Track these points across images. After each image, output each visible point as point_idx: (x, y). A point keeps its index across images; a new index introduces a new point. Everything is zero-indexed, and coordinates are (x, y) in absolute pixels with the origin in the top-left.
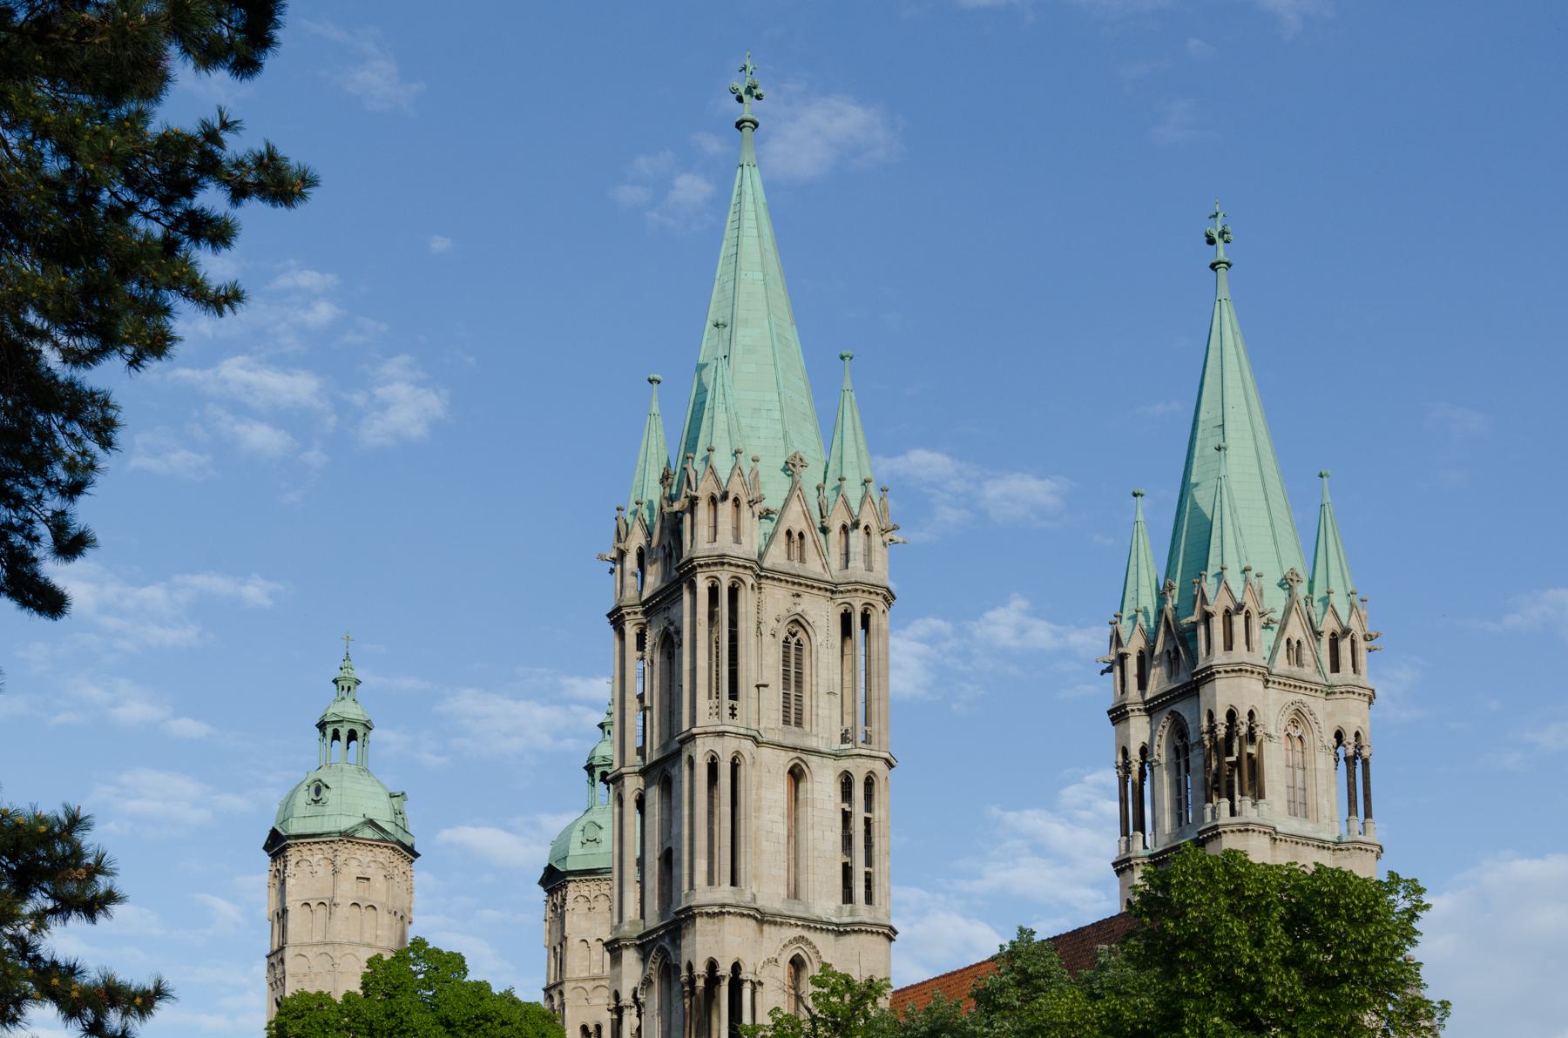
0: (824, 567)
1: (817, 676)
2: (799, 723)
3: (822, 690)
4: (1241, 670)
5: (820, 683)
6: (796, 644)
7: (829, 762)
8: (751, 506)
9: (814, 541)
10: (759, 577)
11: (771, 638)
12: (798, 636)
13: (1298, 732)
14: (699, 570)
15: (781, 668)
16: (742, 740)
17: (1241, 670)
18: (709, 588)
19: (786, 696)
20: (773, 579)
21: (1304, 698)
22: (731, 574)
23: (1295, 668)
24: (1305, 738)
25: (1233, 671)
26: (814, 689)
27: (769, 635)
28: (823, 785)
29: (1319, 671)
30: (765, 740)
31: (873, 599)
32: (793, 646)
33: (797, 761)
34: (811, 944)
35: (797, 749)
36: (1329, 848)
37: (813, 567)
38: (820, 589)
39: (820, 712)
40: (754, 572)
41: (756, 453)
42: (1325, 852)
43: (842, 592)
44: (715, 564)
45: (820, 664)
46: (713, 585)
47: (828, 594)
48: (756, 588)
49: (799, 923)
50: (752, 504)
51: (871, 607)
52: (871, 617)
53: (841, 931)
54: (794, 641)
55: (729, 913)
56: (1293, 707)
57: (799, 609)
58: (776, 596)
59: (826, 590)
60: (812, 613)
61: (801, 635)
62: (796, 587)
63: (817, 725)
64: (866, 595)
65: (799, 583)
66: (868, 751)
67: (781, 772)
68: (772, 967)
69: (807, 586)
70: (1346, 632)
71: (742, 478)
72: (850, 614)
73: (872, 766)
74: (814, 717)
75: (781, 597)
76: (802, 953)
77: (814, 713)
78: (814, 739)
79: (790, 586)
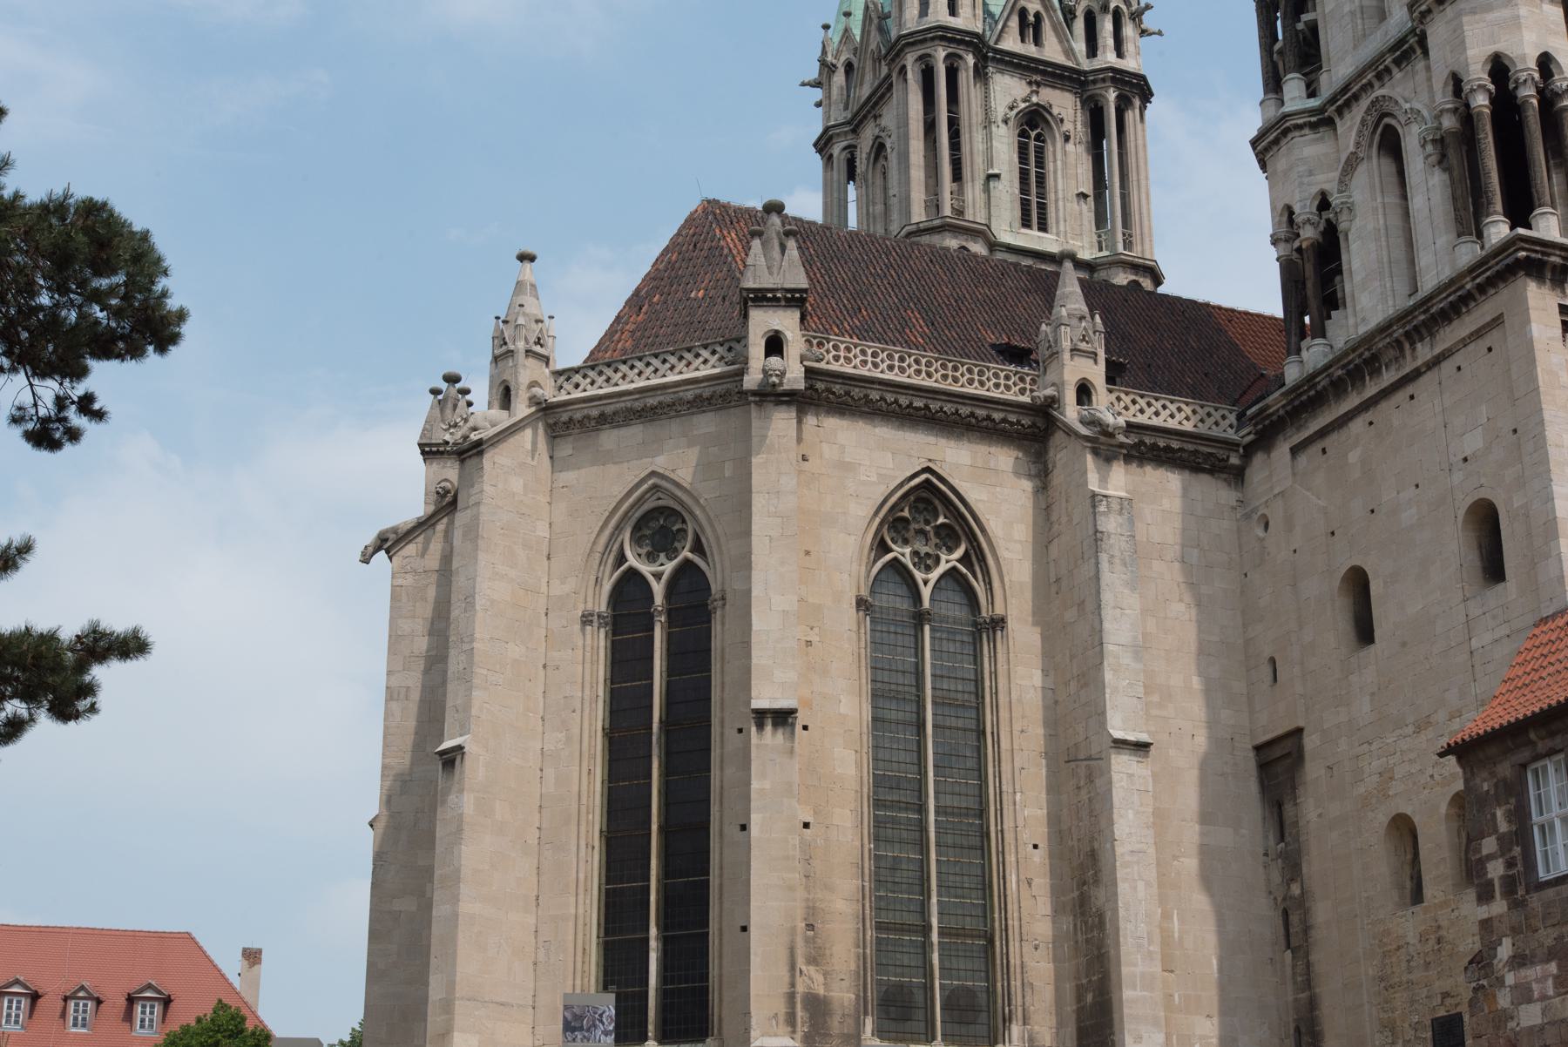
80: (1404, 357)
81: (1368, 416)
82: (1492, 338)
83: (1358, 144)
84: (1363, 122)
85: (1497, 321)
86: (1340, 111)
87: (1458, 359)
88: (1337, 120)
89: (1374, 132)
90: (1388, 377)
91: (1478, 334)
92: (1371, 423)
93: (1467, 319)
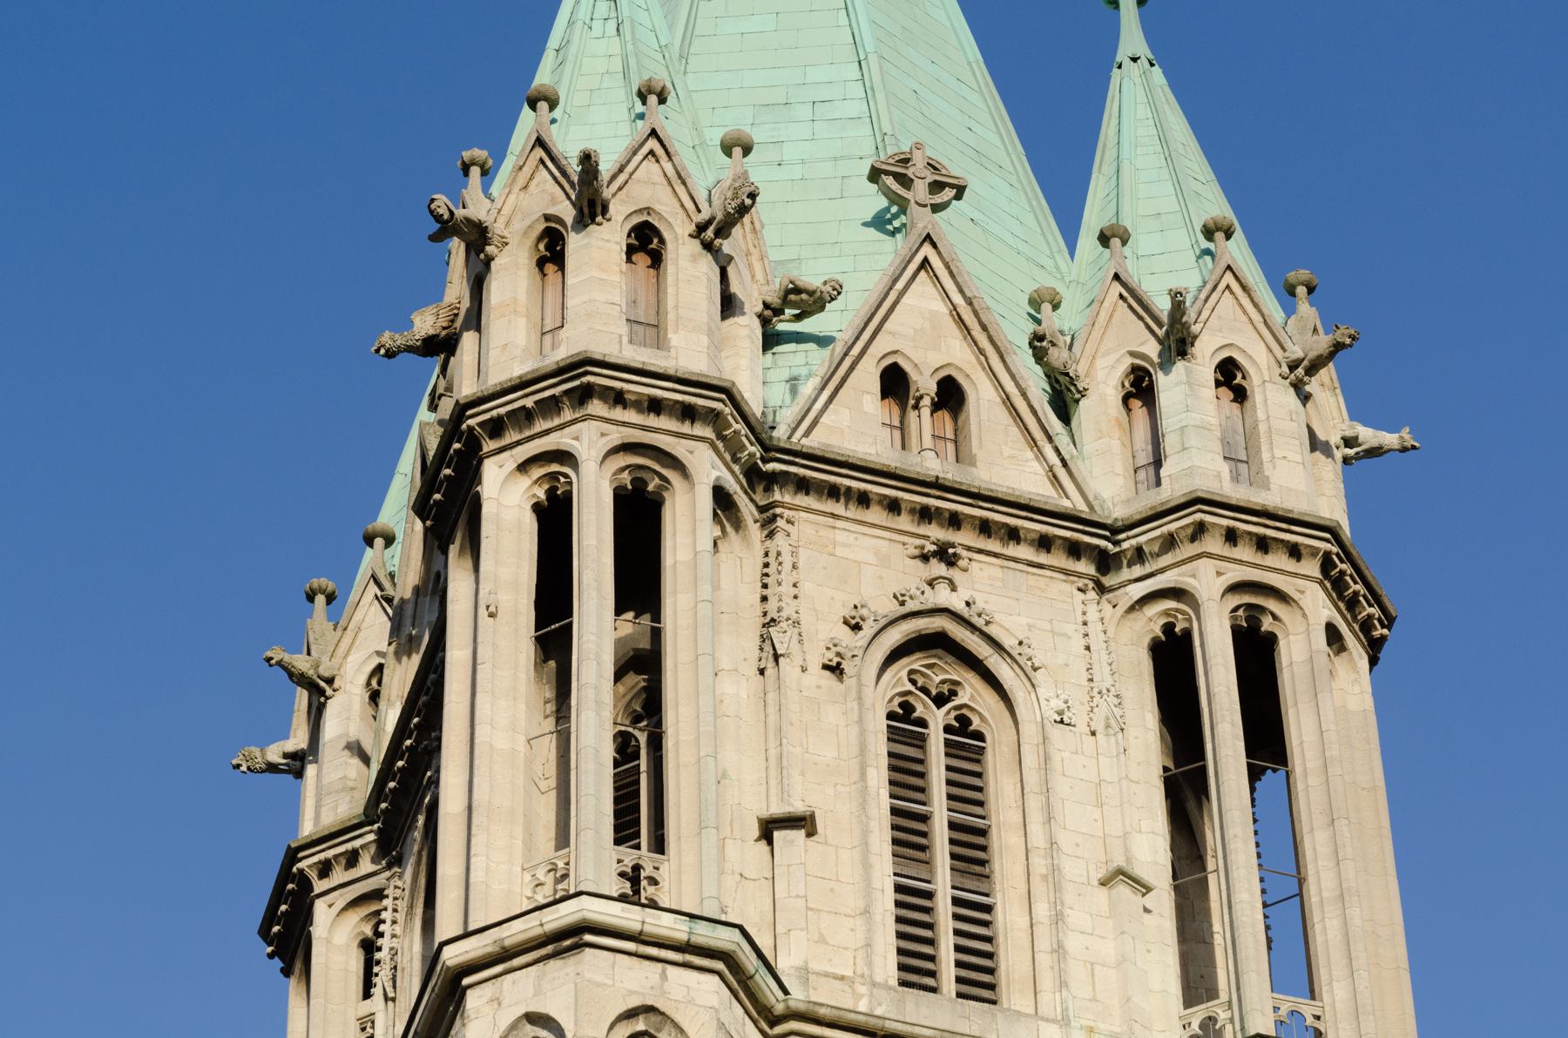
0: (1055, 479)
1: (1049, 819)
3: (1081, 868)
5: (1063, 839)
6: (948, 729)
8: (708, 246)
9: (1007, 401)
14: (489, 445)
15: (881, 801)
16: (672, 971)
18: (537, 508)
22: (617, 436)
26: (1039, 865)
30: (799, 997)
31: (1275, 569)
32: (936, 740)
38: (1045, 543)
39: (1073, 943)
41: (737, 121)
43: (1139, 555)
44: (550, 406)
45: (1061, 786)
46: (551, 492)
47: (1086, 567)
48: (755, 531)
50: (710, 233)
51: (1272, 604)
52: (1282, 644)
58: (839, 551)
61: (972, 692)
62: (936, 532)
63: (1063, 984)
64: (1245, 552)
69: (985, 528)
71: (668, 167)
72: (1187, 634)
74: (1044, 960)
75: (871, 558)
77: (1044, 942)
79: (904, 522)
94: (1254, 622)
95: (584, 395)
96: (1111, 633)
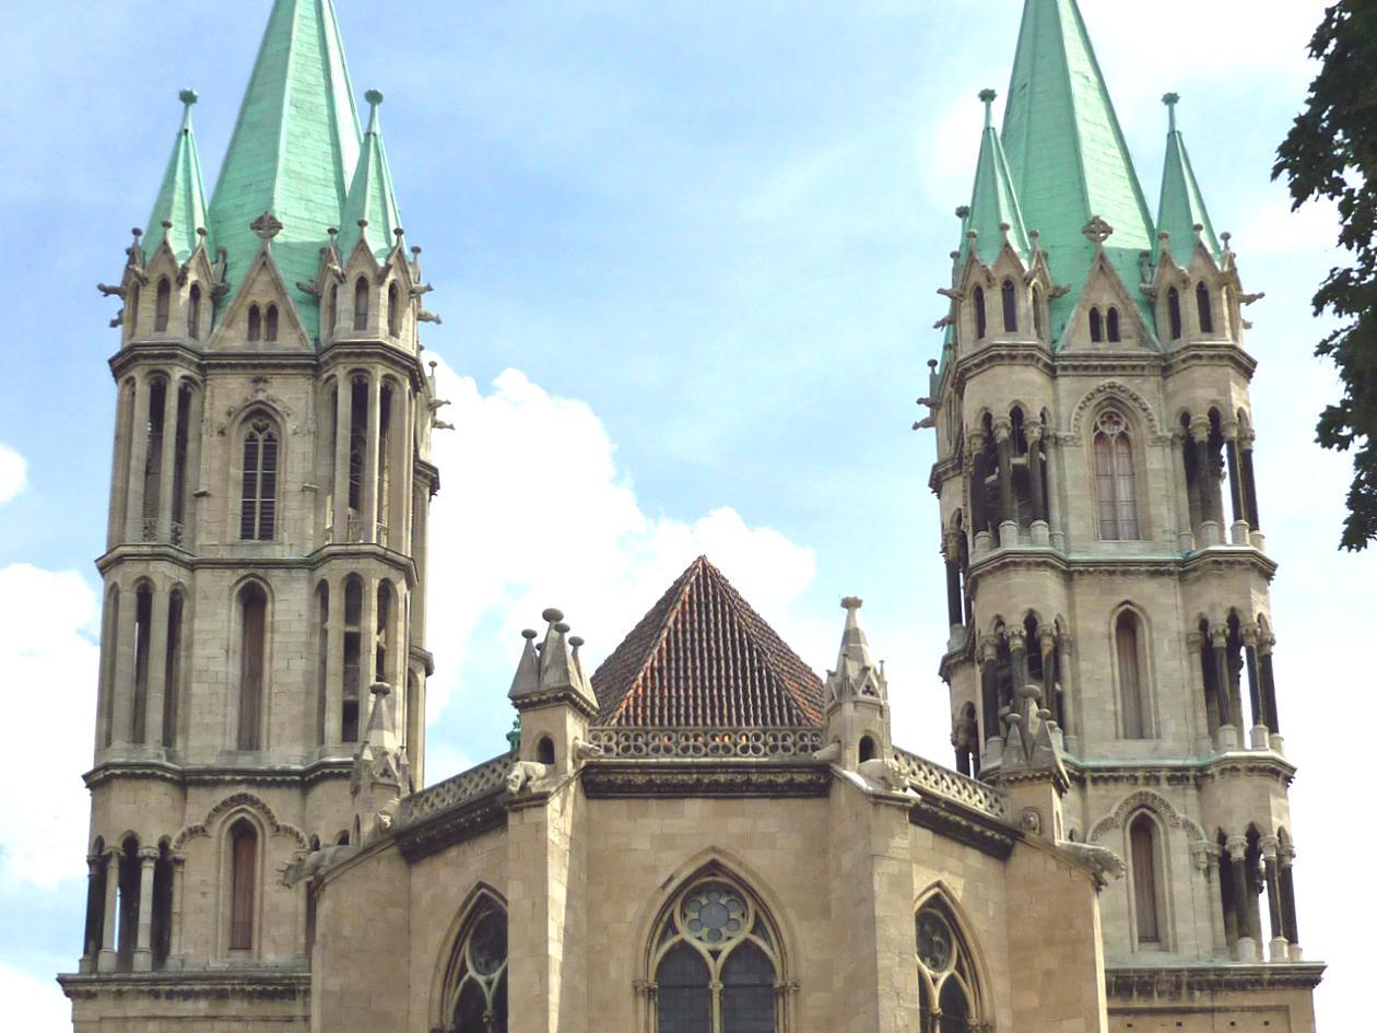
2: (268, 533)
4: (991, 359)
7: (303, 574)
10: (199, 366)
11: (216, 438)
12: (270, 429)
13: (1117, 430)
17: (991, 359)
19: (248, 509)
20: (223, 366)
21: (1118, 381)
22: (147, 369)
23: (1104, 347)
24: (1131, 434)
25: (983, 362)
27: (215, 434)
28: (290, 605)
29: (1144, 342)
33: (251, 579)
34: (258, 802)
35: (249, 564)
36: (1170, 573)
37: (287, 341)
40: (191, 362)
42: (1166, 580)
43: (326, 363)
47: (310, 371)
49: (239, 778)
51: (366, 375)
53: (306, 781)
54: (261, 437)
55: (117, 777)
56: (1100, 397)
57: (261, 396)
59: (305, 366)
60: (285, 398)
65: (259, 367)
66: (344, 548)
67: (225, 595)
68: (199, 839)
70: (1185, 281)
73: (354, 566)
76: (247, 817)
78: (278, 548)
80: (1179, 994)
81: (1129, 1019)
82: (1272, 1017)
83: (1117, 814)
84: (1126, 802)
85: (1283, 1010)
86: (1095, 781)
87: (1235, 1017)
88: (1089, 785)
89: (1131, 812)
90: (1158, 1002)
91: (1258, 1010)
92: (1129, 1026)
93: (1252, 995)
94: (360, 381)
95: (135, 358)
96: (319, 390)
